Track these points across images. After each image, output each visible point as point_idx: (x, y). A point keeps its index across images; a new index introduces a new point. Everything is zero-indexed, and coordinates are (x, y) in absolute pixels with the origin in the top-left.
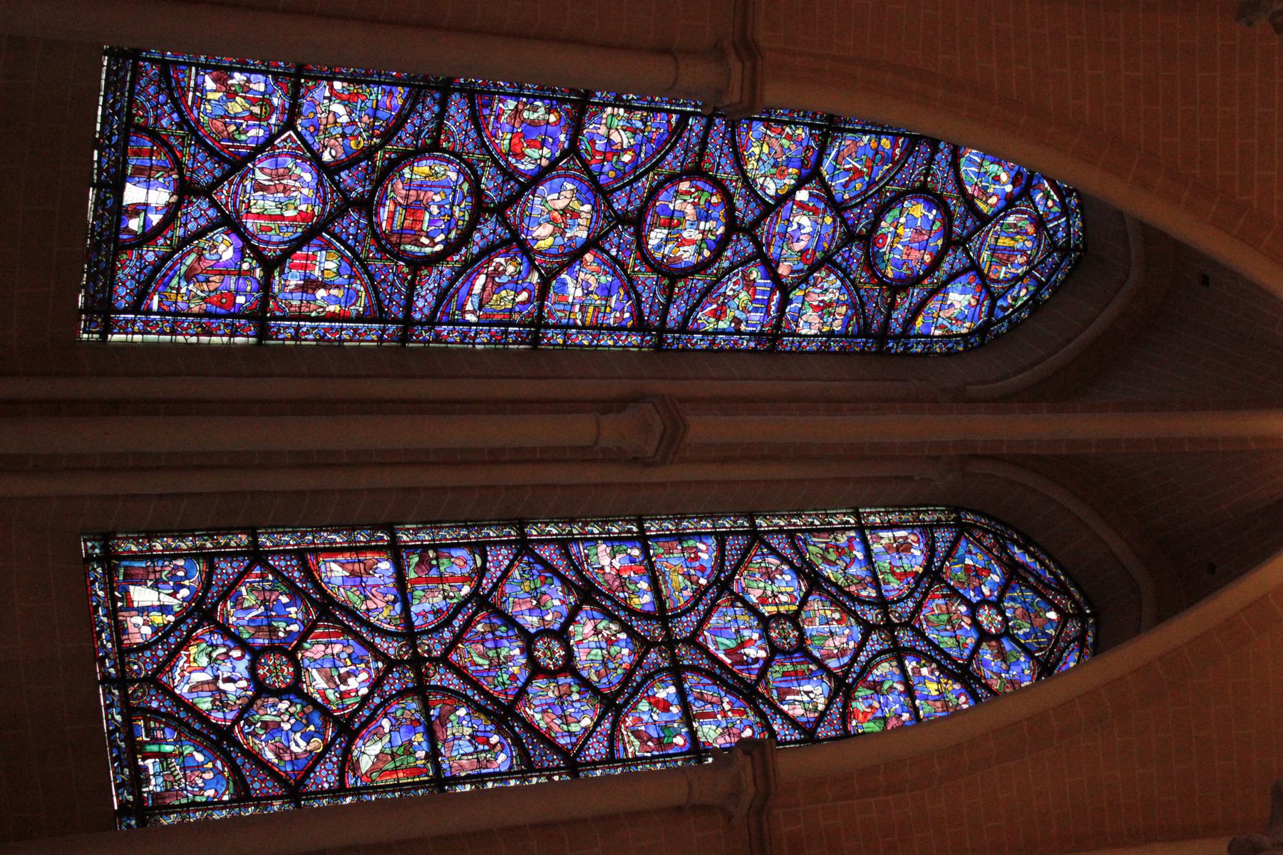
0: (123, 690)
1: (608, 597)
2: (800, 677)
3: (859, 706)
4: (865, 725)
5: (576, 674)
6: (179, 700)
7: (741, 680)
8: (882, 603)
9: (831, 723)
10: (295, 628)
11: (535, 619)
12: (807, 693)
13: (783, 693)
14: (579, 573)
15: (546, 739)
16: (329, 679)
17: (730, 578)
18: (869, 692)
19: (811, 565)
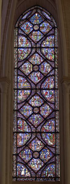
0: (37, 178)
1: (27, 98)
2: (44, 68)
5: (40, 107)
6: (40, 170)
7: (43, 78)
8: (32, 48)
9: (52, 64)
10: (29, 151)
12: (47, 67)
13: (46, 71)
16: (38, 147)
17: (26, 75)
19: (24, 59)
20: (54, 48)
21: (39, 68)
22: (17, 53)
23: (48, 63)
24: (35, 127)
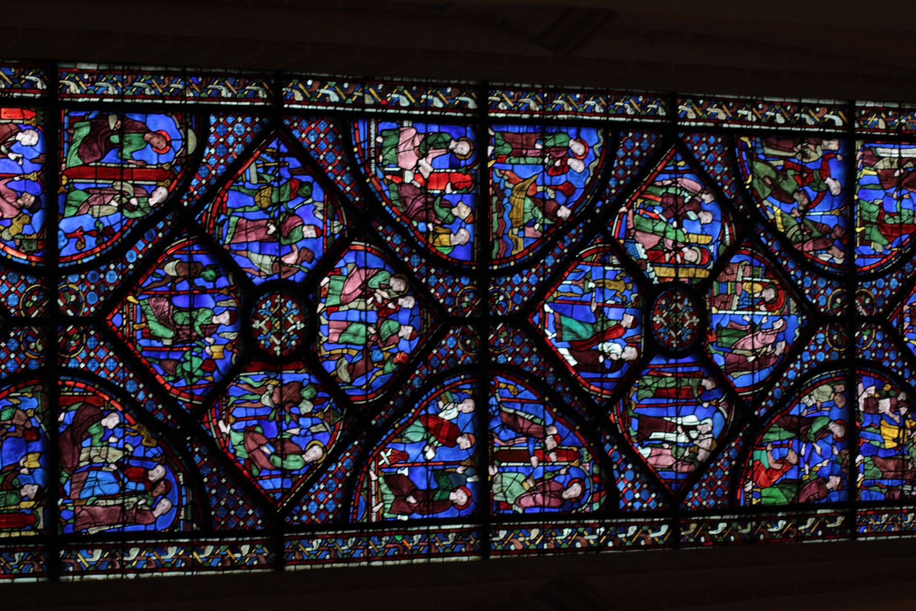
1: (398, 229)
2: (684, 399)
3: (765, 458)
4: (765, 492)
7: (586, 398)
8: (848, 277)
11: (267, 260)
12: (687, 429)
13: (649, 425)
14: (359, 179)
15: (240, 476)
17: (611, 212)
18: (786, 435)
19: (751, 197)
20: (850, 502)
21: (677, 354)
22: (802, 123)
23: (721, 442)
24: (105, 309)
